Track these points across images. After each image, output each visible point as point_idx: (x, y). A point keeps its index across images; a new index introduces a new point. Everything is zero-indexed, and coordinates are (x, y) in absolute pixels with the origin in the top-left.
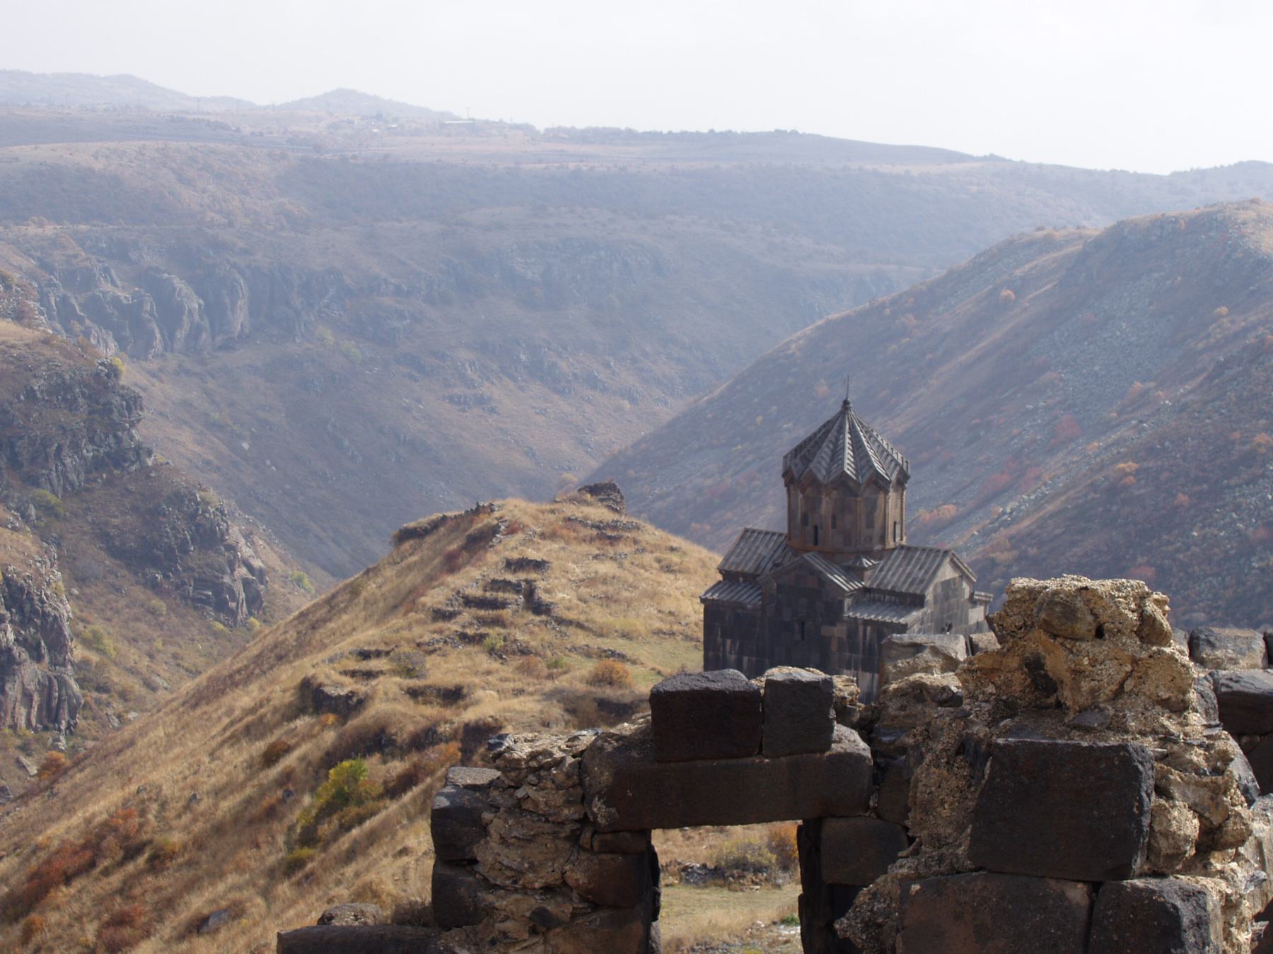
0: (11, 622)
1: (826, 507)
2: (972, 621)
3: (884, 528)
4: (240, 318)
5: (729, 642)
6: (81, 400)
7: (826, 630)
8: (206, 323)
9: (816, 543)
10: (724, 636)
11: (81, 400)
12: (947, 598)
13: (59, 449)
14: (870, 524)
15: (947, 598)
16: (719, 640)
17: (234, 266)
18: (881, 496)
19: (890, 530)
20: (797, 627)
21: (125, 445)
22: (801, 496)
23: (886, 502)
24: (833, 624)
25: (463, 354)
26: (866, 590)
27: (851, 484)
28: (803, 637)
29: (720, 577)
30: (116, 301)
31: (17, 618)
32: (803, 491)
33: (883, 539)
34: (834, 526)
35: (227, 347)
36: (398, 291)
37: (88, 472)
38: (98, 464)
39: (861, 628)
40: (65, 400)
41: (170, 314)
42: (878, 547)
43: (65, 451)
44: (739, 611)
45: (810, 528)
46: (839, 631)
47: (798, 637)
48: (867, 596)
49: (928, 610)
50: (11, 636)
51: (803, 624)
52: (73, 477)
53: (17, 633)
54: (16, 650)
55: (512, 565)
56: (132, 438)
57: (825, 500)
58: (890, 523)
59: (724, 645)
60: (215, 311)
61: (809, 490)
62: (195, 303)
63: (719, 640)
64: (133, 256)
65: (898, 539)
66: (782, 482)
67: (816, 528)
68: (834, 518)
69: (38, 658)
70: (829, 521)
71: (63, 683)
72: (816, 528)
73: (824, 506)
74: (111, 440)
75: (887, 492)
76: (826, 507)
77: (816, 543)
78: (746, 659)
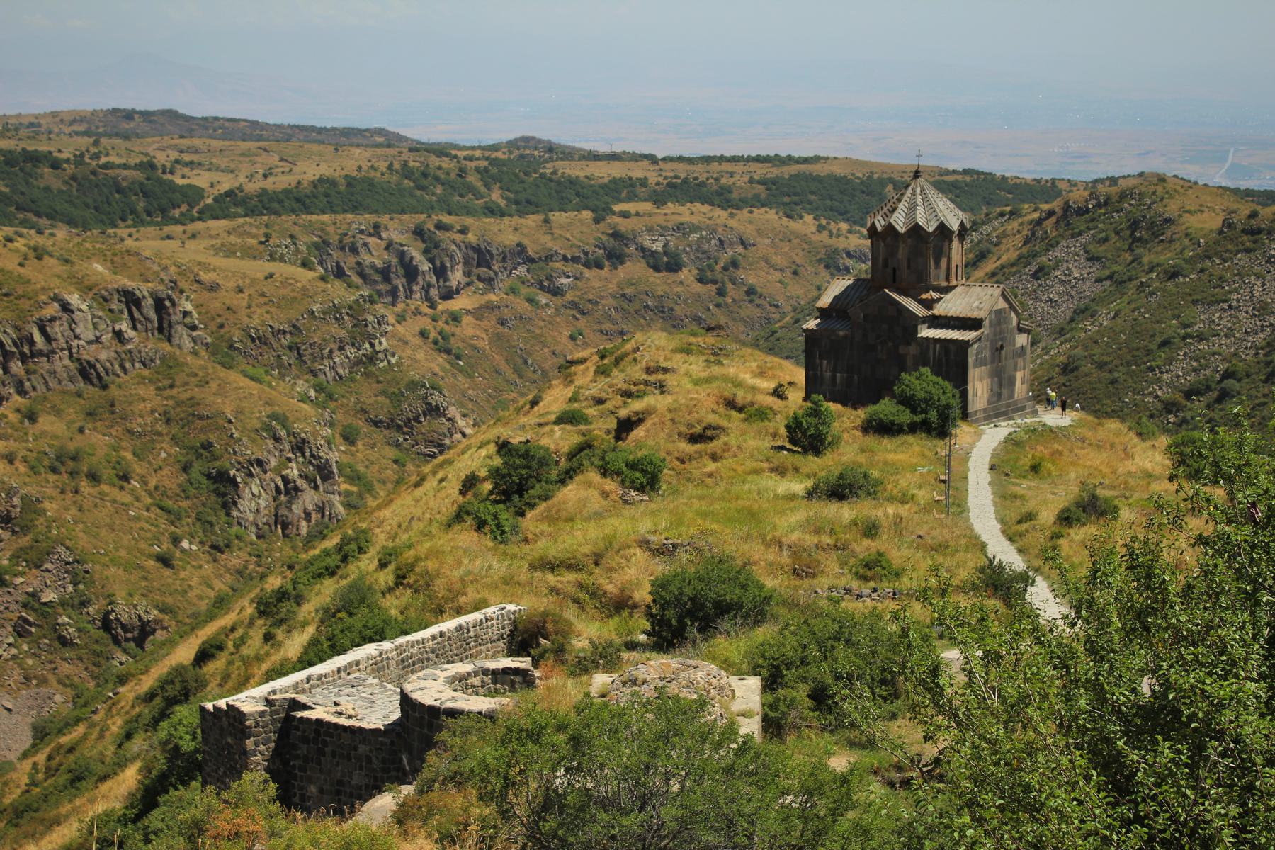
0: (297, 462)
1: (902, 252)
2: (1018, 345)
4: (457, 277)
5: (825, 362)
6: (346, 318)
7: (902, 350)
8: (434, 280)
9: (894, 281)
11: (346, 318)
12: (999, 324)
13: (331, 351)
15: (999, 324)
16: (818, 361)
17: (454, 242)
18: (947, 243)
19: (953, 270)
21: (377, 348)
23: (950, 248)
24: (909, 344)
25: (610, 301)
26: (934, 317)
30: (373, 266)
31: (301, 459)
33: (948, 279)
34: (909, 267)
35: (448, 295)
36: (565, 258)
37: (351, 368)
38: (359, 362)
40: (336, 319)
41: (411, 273)
42: (944, 284)
43: (337, 353)
45: (889, 270)
46: (913, 349)
48: (936, 322)
49: (985, 330)
50: (296, 472)
52: (340, 371)
53: (300, 470)
54: (300, 482)
55: (648, 371)
56: (381, 343)
57: (902, 246)
59: (821, 365)
60: (441, 272)
61: (889, 239)
62: (425, 266)
63: (818, 361)
64: (384, 235)
67: (894, 270)
69: (316, 488)
70: (905, 265)
71: (331, 504)
72: (894, 270)
73: (901, 251)
74: (367, 345)
75: (951, 241)
76: (902, 252)
77: (894, 281)
78: (838, 375)
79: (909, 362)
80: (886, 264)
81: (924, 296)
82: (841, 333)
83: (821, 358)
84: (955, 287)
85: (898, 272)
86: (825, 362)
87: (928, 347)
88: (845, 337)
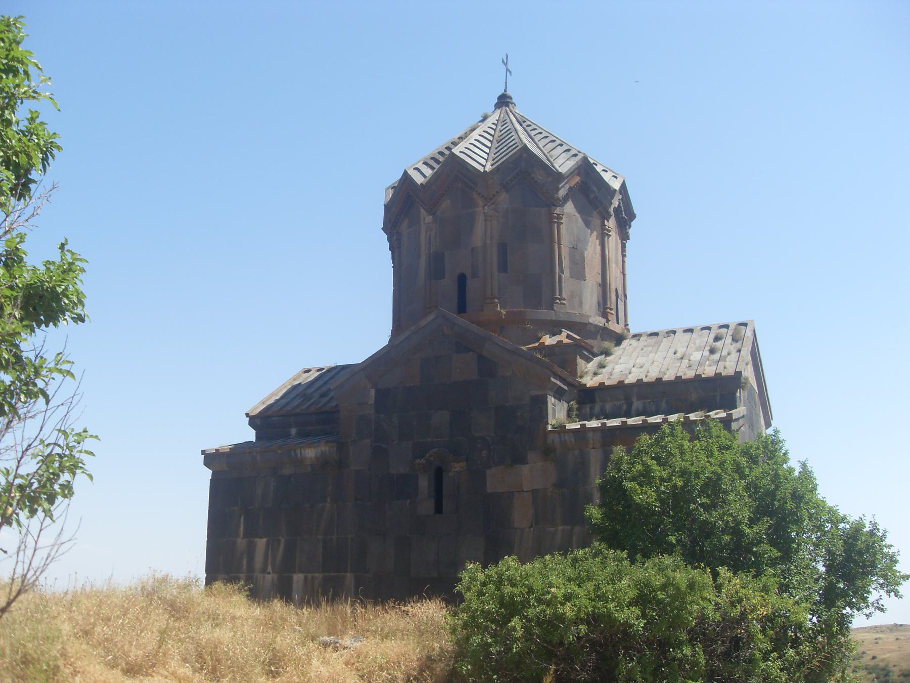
1: (483, 231)
3: (604, 285)
5: (261, 543)
7: (496, 480)
9: (462, 308)
10: (250, 534)
14: (579, 273)
16: (241, 542)
20: (424, 483)
22: (429, 219)
24: (520, 459)
27: (539, 176)
28: (439, 509)
29: (250, 435)
32: (431, 211)
34: (503, 267)
39: (595, 457)
44: (287, 471)
45: (449, 284)
46: (533, 475)
47: (426, 507)
51: (439, 475)
58: (613, 288)
59: (250, 551)
61: (446, 204)
63: (241, 542)
67: (462, 280)
68: (503, 250)
72: (462, 280)
76: (483, 231)
79: (521, 516)
81: (548, 340)
82: (310, 453)
83: (250, 534)
84: (619, 339)
85: (472, 285)
86: (261, 543)
87: (583, 464)
88: (323, 463)
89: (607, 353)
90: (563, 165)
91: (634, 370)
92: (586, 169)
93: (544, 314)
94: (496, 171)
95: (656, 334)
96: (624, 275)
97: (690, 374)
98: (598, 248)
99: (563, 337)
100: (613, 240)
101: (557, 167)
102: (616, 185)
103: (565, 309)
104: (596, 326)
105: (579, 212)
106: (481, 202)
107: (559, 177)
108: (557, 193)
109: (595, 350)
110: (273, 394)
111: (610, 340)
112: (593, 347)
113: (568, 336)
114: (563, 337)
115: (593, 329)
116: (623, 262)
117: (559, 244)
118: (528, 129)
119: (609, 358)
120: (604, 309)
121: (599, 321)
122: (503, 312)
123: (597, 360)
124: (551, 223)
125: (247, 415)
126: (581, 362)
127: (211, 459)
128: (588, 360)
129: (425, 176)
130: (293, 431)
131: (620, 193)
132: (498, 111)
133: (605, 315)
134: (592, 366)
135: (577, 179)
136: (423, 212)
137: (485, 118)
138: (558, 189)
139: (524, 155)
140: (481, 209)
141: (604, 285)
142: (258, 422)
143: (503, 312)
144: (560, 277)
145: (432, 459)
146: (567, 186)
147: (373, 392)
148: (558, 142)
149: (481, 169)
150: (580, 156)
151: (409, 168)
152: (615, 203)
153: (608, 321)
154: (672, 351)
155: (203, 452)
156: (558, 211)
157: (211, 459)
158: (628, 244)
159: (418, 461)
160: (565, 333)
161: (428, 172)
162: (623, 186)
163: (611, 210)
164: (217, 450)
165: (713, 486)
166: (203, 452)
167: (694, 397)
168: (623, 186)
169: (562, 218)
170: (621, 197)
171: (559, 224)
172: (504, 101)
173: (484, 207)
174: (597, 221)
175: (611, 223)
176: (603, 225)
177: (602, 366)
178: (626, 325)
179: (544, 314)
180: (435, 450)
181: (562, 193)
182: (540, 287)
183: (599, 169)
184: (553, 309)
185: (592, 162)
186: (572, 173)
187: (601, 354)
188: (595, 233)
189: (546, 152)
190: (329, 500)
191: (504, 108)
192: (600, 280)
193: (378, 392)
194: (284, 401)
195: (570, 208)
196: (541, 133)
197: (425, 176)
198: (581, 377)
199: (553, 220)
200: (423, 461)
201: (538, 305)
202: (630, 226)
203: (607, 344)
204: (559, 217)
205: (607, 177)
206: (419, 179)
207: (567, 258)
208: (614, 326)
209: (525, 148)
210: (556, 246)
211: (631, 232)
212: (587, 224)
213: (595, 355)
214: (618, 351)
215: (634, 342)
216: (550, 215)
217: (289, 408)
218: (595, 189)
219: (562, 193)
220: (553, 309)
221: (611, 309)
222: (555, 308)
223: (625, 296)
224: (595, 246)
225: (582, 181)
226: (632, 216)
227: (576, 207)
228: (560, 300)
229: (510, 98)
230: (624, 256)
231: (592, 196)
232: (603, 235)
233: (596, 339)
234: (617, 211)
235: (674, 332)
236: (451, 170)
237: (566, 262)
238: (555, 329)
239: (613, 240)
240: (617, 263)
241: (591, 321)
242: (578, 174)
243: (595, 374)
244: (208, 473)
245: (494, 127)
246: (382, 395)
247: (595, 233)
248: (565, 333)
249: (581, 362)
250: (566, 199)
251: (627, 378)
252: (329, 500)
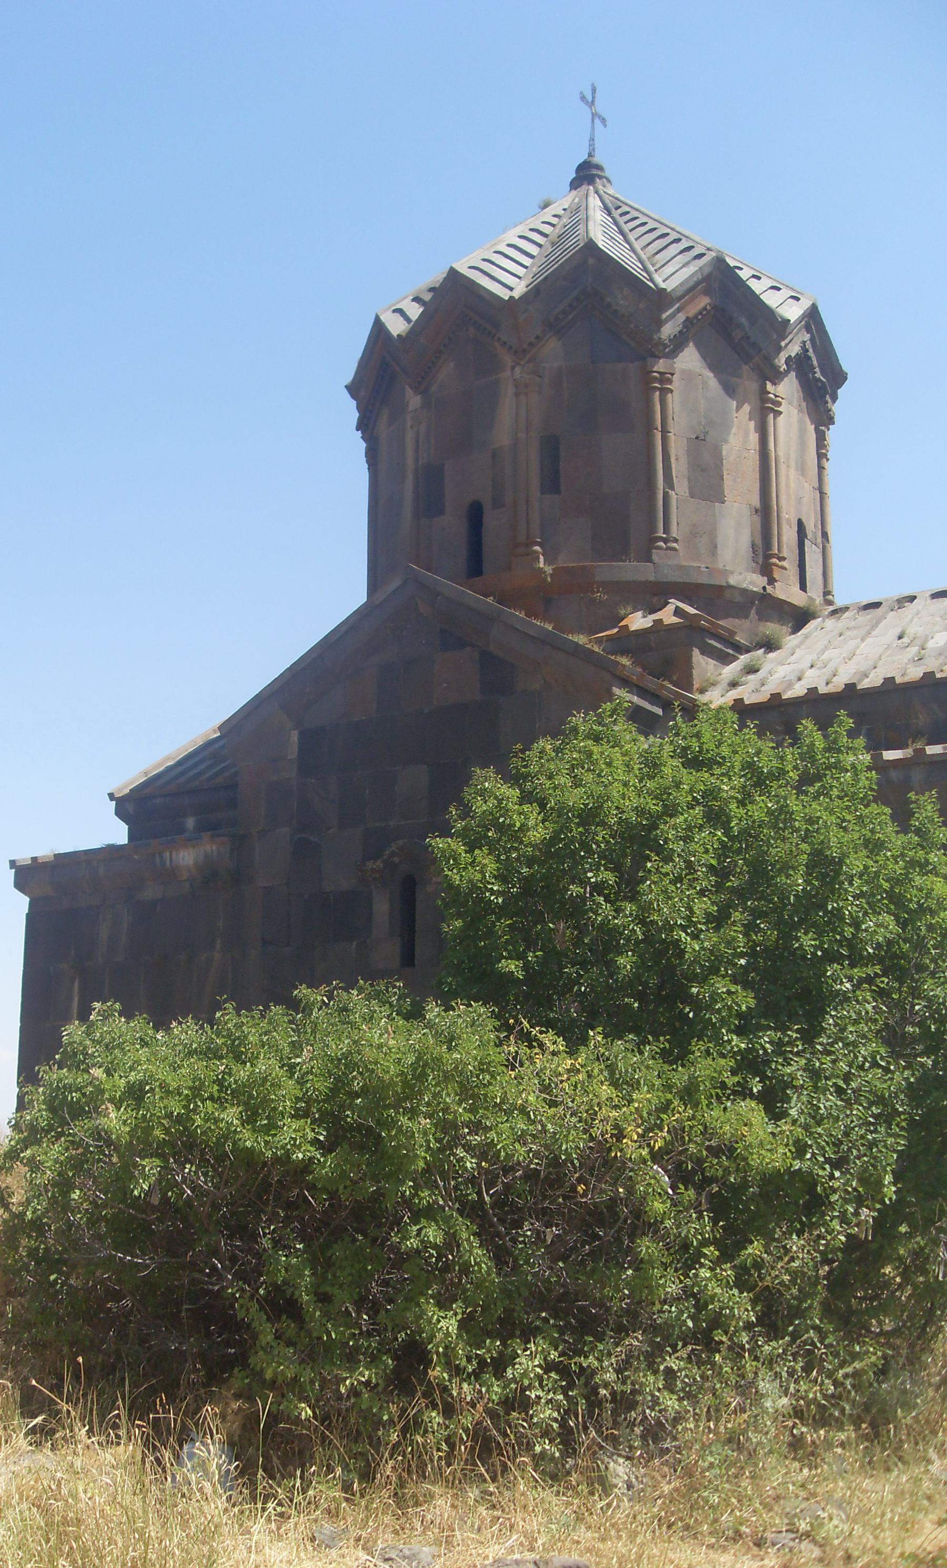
1: (514, 419)
3: (765, 512)
14: (709, 485)
20: (382, 907)
22: (414, 401)
27: (622, 300)
32: (421, 387)
34: (552, 482)
44: (150, 892)
45: (451, 524)
57: (512, 374)
61: (447, 371)
65: (815, 592)
66: (350, 411)
68: (551, 448)
76: (514, 419)
80: (430, 503)
81: (638, 621)
82: (186, 858)
85: (493, 522)
88: (209, 875)
89: (770, 645)
90: (671, 275)
91: (810, 673)
92: (722, 281)
93: (632, 570)
94: (535, 293)
95: (876, 605)
96: (822, 494)
97: (915, 673)
98: (754, 438)
99: (667, 616)
100: (790, 422)
101: (659, 279)
102: (793, 313)
103: (677, 560)
104: (744, 591)
105: (711, 367)
106: (508, 360)
107: (661, 298)
108: (658, 330)
109: (740, 638)
110: (168, 759)
111: (781, 621)
112: (733, 633)
113: (678, 612)
114: (667, 616)
115: (738, 598)
116: (821, 468)
117: (665, 432)
118: (621, 220)
119: (771, 655)
120: (765, 559)
121: (754, 582)
122: (549, 570)
123: (744, 659)
124: (648, 391)
125: (111, 796)
126: (703, 665)
127: (27, 875)
128: (725, 659)
129: (408, 320)
130: (190, 823)
131: (808, 328)
132: (574, 193)
133: (766, 570)
134: (729, 671)
135: (704, 301)
136: (409, 391)
137: (546, 205)
138: (660, 324)
139: (591, 261)
140: (508, 373)
141: (765, 512)
142: (130, 808)
143: (549, 570)
144: (666, 497)
145: (396, 860)
146: (681, 317)
147: (295, 736)
148: (674, 235)
149: (505, 294)
150: (711, 255)
151: (385, 311)
152: (794, 350)
153: (772, 581)
154: (898, 631)
155: (13, 864)
156: (661, 365)
157: (27, 875)
158: (832, 434)
159: (370, 865)
160: (674, 603)
161: (415, 311)
162: (813, 318)
163: (781, 361)
164: (34, 859)
165: (639, 843)
166: (13, 864)
167: (922, 720)
168: (813, 318)
169: (670, 381)
170: (807, 337)
171: (664, 392)
172: (587, 174)
173: (513, 368)
174: (751, 386)
175: (787, 390)
176: (764, 392)
177: (751, 670)
178: (827, 593)
179: (632, 570)
180: (401, 842)
181: (668, 330)
182: (623, 517)
183: (744, 274)
184: (649, 560)
185: (732, 263)
186: (691, 289)
187: (759, 646)
188: (746, 408)
189: (644, 257)
190: (218, 945)
191: (584, 187)
192: (756, 502)
193: (302, 734)
194: (180, 769)
195: (689, 359)
196: (644, 224)
197: (408, 320)
198: (702, 691)
199: (654, 385)
200: (379, 864)
201: (621, 552)
202: (834, 398)
203: (771, 628)
204: (665, 378)
205: (771, 300)
206: (396, 327)
207: (683, 460)
208: (787, 590)
209: (591, 246)
210: (659, 435)
211: (838, 409)
212: (730, 390)
213: (740, 649)
214: (790, 641)
215: (830, 623)
216: (646, 377)
217: (181, 780)
218: (743, 320)
219: (668, 330)
220: (649, 560)
221: (782, 559)
222: (655, 558)
223: (825, 535)
224: (747, 434)
225: (714, 307)
226: (838, 377)
227: (704, 357)
228: (665, 541)
229: (599, 167)
230: (821, 456)
231: (737, 335)
232: (765, 410)
233: (747, 617)
234: (800, 364)
235: (912, 599)
236: (457, 305)
237: (679, 467)
238: (655, 600)
239: (790, 422)
240: (802, 469)
241: (732, 581)
242: (707, 292)
243: (734, 684)
244: (21, 903)
245: (555, 221)
246: (312, 739)
247: (746, 408)
248: (674, 603)
249: (703, 665)
250: (678, 343)
251: (790, 685)
252: (218, 945)
